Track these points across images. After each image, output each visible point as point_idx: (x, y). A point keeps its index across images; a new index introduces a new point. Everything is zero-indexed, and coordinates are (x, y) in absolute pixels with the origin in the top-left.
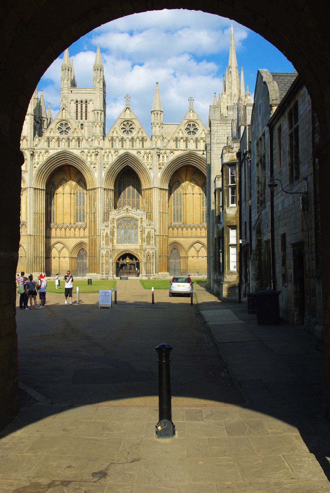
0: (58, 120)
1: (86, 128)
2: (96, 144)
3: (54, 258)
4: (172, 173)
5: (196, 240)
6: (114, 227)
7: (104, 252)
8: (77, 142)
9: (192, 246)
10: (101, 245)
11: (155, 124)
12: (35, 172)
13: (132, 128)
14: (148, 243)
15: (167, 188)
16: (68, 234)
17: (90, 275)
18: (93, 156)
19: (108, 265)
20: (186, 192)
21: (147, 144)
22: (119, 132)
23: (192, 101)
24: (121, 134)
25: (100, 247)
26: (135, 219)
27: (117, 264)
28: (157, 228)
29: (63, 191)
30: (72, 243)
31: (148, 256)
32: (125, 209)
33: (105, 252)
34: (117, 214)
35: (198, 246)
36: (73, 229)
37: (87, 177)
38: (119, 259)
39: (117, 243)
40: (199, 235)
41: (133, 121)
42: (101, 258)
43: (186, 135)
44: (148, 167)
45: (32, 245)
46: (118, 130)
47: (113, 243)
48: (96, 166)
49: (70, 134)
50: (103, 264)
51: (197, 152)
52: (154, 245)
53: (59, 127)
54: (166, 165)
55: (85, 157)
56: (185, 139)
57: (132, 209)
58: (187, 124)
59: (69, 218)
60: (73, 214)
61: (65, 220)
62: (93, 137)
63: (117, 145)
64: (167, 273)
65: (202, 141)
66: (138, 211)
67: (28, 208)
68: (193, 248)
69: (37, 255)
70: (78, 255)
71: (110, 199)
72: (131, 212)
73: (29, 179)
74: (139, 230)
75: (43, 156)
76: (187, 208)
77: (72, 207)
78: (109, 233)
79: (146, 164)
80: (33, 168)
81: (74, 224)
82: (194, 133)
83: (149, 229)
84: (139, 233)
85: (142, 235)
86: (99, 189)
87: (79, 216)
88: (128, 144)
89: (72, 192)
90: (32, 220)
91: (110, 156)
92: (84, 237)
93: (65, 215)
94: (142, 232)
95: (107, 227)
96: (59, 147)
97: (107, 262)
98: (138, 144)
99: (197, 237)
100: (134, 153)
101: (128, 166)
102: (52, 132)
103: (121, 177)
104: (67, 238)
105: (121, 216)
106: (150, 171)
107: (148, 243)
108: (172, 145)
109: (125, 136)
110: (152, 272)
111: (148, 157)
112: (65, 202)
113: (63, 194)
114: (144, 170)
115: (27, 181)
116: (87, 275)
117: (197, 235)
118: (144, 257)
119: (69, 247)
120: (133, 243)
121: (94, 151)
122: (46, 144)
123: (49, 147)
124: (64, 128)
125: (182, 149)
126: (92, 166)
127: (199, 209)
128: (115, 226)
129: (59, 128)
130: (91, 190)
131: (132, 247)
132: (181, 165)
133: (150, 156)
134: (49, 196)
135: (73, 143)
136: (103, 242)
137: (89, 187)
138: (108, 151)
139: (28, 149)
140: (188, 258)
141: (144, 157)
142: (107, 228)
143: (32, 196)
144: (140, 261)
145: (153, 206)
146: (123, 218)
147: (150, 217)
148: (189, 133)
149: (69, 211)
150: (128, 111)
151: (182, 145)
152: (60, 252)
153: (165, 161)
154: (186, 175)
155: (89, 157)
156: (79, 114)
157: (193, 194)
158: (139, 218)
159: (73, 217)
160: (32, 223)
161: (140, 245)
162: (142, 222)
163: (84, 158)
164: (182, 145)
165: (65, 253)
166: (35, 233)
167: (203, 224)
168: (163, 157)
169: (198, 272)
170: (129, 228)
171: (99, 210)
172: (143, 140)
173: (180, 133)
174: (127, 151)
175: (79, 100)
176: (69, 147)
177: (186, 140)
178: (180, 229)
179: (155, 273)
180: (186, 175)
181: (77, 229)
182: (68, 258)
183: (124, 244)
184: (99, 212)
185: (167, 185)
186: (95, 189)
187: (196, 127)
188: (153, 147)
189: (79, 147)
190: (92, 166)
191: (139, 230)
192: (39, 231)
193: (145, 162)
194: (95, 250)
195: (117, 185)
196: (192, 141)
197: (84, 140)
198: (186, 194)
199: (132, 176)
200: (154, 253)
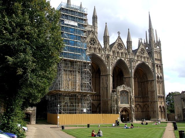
2: (107, 53)
5: (137, 103)
13: (121, 48)
33: (116, 108)
37: (102, 68)
42: (113, 111)
62: (106, 49)
82: (143, 54)
84: (129, 99)
91: (113, 59)
95: (116, 95)
100: (123, 59)
106: (130, 69)
127: (138, 89)
130: (104, 75)
137: (103, 73)
155: (105, 59)
163: (103, 59)
172: (126, 54)
176: (95, 52)
177: (141, 57)
188: (130, 58)
190: (106, 63)
191: (129, 97)
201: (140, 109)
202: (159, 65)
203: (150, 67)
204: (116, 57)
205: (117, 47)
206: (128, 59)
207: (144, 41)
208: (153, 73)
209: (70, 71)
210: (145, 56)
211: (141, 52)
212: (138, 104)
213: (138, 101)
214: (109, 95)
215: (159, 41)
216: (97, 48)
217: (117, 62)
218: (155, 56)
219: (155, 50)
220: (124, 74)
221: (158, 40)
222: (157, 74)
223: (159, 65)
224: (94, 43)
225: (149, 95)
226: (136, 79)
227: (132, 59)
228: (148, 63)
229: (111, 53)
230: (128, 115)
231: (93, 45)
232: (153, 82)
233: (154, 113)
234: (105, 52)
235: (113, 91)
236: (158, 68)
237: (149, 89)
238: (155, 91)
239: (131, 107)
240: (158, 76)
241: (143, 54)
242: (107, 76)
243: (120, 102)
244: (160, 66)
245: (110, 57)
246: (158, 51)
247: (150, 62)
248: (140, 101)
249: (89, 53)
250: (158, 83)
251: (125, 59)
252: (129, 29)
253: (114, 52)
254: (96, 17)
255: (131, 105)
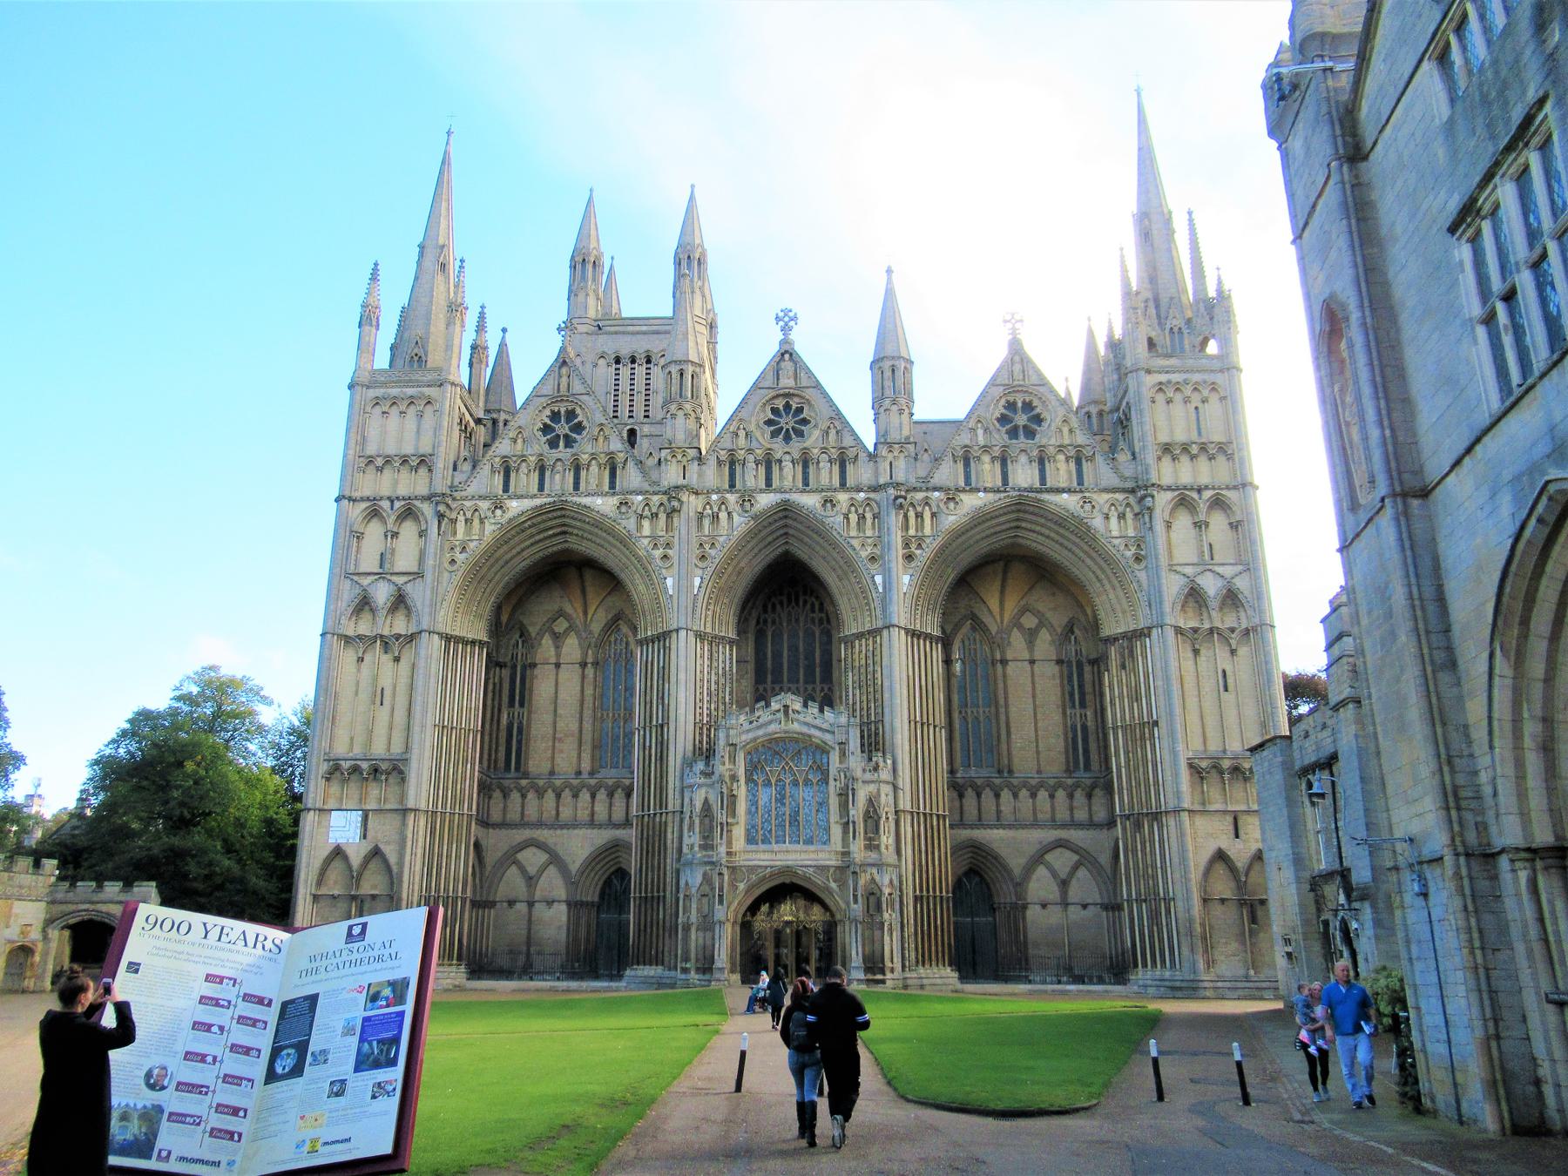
0: (543, 400)
1: (643, 444)
2: (671, 475)
3: (511, 903)
4: (951, 575)
6: (734, 778)
7: (693, 879)
8: (607, 472)
9: (1038, 859)
10: (685, 850)
11: (887, 402)
12: (450, 583)
13: (805, 422)
14: (872, 845)
15: (937, 632)
16: (566, 813)
17: (639, 973)
18: (662, 516)
19: (709, 935)
20: (1003, 653)
21: (861, 473)
22: (758, 434)
23: (1018, 325)
24: (763, 438)
25: (679, 860)
26: (818, 747)
27: (746, 926)
28: (905, 780)
29: (558, 655)
30: (579, 846)
31: (874, 900)
32: (775, 706)
33: (699, 879)
34: (746, 726)
35: (1062, 861)
36: (585, 796)
38: (754, 908)
39: (750, 840)
40: (1062, 814)
41: (809, 393)
43: (1000, 437)
44: (864, 554)
45: (420, 851)
46: (752, 427)
47: (729, 843)
48: (670, 552)
49: (585, 447)
50: (687, 928)
51: (1046, 497)
52: (892, 849)
53: (545, 425)
54: (931, 546)
55: (633, 520)
56: (997, 451)
57: (805, 705)
58: (1003, 402)
59: (574, 754)
60: (587, 737)
61: (558, 760)
62: (664, 453)
63: (752, 477)
64: (949, 969)
65: (1061, 457)
66: (828, 714)
67: (417, 709)
68: (1041, 871)
69: (438, 890)
70: (602, 895)
71: (724, 674)
72: (801, 717)
73: (427, 602)
74: (833, 788)
75: (482, 522)
76: (1013, 715)
77: (588, 713)
78: (713, 798)
79: (855, 543)
80: (446, 565)
81: (592, 774)
82: (1030, 434)
83: (872, 788)
84: (834, 802)
85: (844, 807)
86: (683, 633)
87: (610, 744)
88: (788, 474)
89: (590, 660)
90: (428, 754)
91: (723, 515)
92: (627, 823)
93: (560, 740)
94: (846, 796)
95: (707, 774)
96: (541, 488)
97: (708, 924)
98: (826, 474)
99: (1054, 824)
100: (810, 501)
101: (786, 554)
102: (520, 441)
103: (765, 611)
104: (562, 827)
105: (760, 732)
106: (874, 568)
107: (872, 845)
108: (949, 473)
109: (778, 447)
110: (888, 964)
111: (862, 517)
112: (561, 696)
113: (558, 665)
114: (848, 566)
115: (419, 604)
116: (628, 972)
117: (1058, 816)
118: (856, 901)
119: (568, 859)
120: (809, 842)
121: (665, 498)
122: (498, 480)
123: (506, 489)
124: (562, 428)
125: (989, 485)
126: (658, 553)
127: (1057, 717)
128: (741, 772)
129: (546, 429)
131: (804, 856)
132: (983, 547)
133: (869, 516)
134: (506, 673)
135: (594, 476)
136: (692, 839)
138: (714, 497)
139: (429, 498)
140: (1025, 907)
141: (846, 517)
142: (708, 781)
143: (436, 666)
144: (838, 917)
145: (886, 695)
146: (770, 741)
147: (874, 742)
148: (1013, 433)
149: (574, 726)
150: (787, 365)
151: (988, 472)
152: (531, 881)
153: (927, 530)
154: (1002, 592)
155: (646, 523)
156: (624, 400)
157: (1032, 662)
158: (828, 737)
159: (587, 748)
160: (427, 763)
161: (840, 849)
162: (843, 755)
163: (631, 524)
164: (988, 472)
165: (553, 885)
166: (435, 804)
167: (1081, 773)
168: (919, 516)
169: (1069, 970)
170: (795, 783)
171: (681, 711)
173: (980, 432)
174: (787, 496)
175: (625, 352)
176: (576, 486)
178: (987, 795)
179: (903, 967)
180: (1002, 592)
181: (602, 795)
182: (564, 907)
183: (775, 847)
184: (681, 719)
185: (937, 620)
186: (663, 637)
187: (1038, 410)
188: (882, 481)
189: (612, 485)
190: (658, 553)
191: (833, 788)
192: (454, 797)
193: (853, 533)
194: (661, 868)
195: (751, 638)
196: (1023, 459)
197: (630, 464)
198: (1004, 662)
199: (805, 602)
200: (896, 882)
201: (1085, 887)
202: (1207, 494)
203: (1097, 522)
204: (747, 499)
205: (769, 423)
206: (859, 490)
207: (1111, 329)
208: (1142, 576)
209: (386, 646)
210: (1044, 442)
211: (1003, 419)
212: (1061, 844)
213: (1062, 814)
214: (672, 782)
215: (1220, 291)
216: (594, 457)
217: (751, 534)
218: (1162, 421)
219: (1163, 378)
220: (844, 605)
221: (1212, 293)
222: (1189, 570)
223: (1207, 494)
224: (578, 428)
225: (1119, 762)
226: (1044, 636)
227: (897, 485)
228: (1069, 491)
229: (712, 476)
230: (831, 928)
231: (569, 442)
232: (1144, 647)
233: (1154, 916)
234: (654, 476)
235: (706, 752)
236: (1198, 525)
237: (1118, 711)
238: (1156, 723)
239: (846, 869)
240: (1194, 595)
241: (1030, 434)
242: (663, 637)
243: (739, 832)
244: (1218, 503)
245: (693, 503)
246: (1197, 377)
247: (1108, 477)
248: (1081, 815)
249: (538, 502)
250: (1196, 652)
251: (828, 502)
252: (889, 271)
253: (732, 463)
254: (703, 254)
255: (846, 854)
